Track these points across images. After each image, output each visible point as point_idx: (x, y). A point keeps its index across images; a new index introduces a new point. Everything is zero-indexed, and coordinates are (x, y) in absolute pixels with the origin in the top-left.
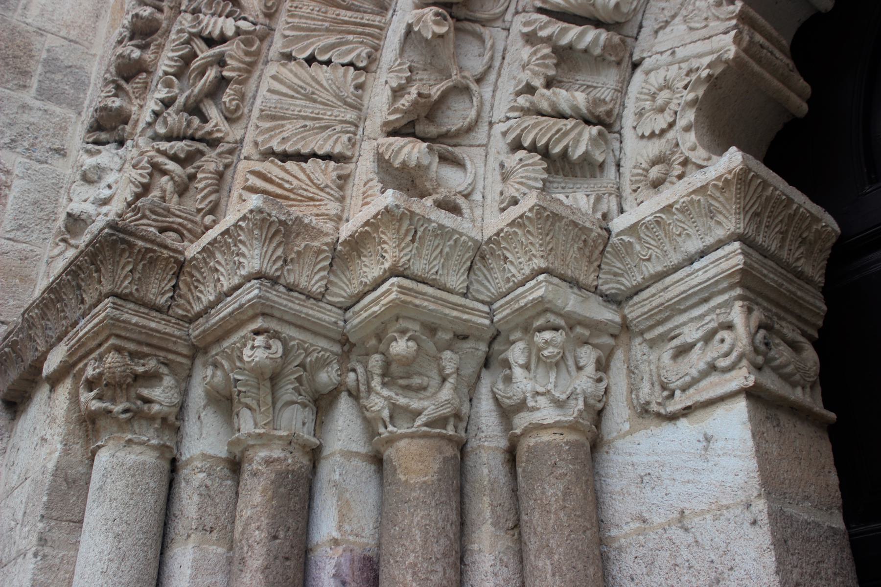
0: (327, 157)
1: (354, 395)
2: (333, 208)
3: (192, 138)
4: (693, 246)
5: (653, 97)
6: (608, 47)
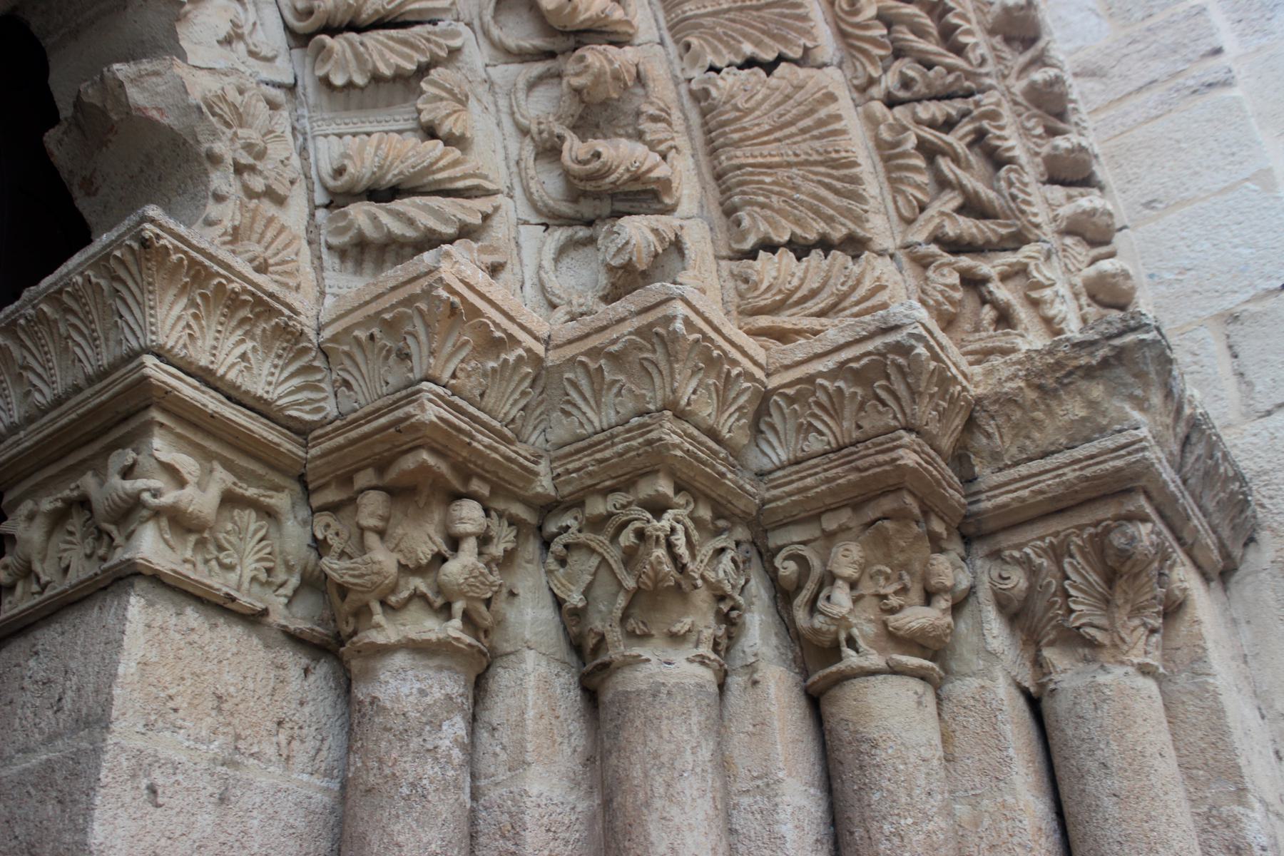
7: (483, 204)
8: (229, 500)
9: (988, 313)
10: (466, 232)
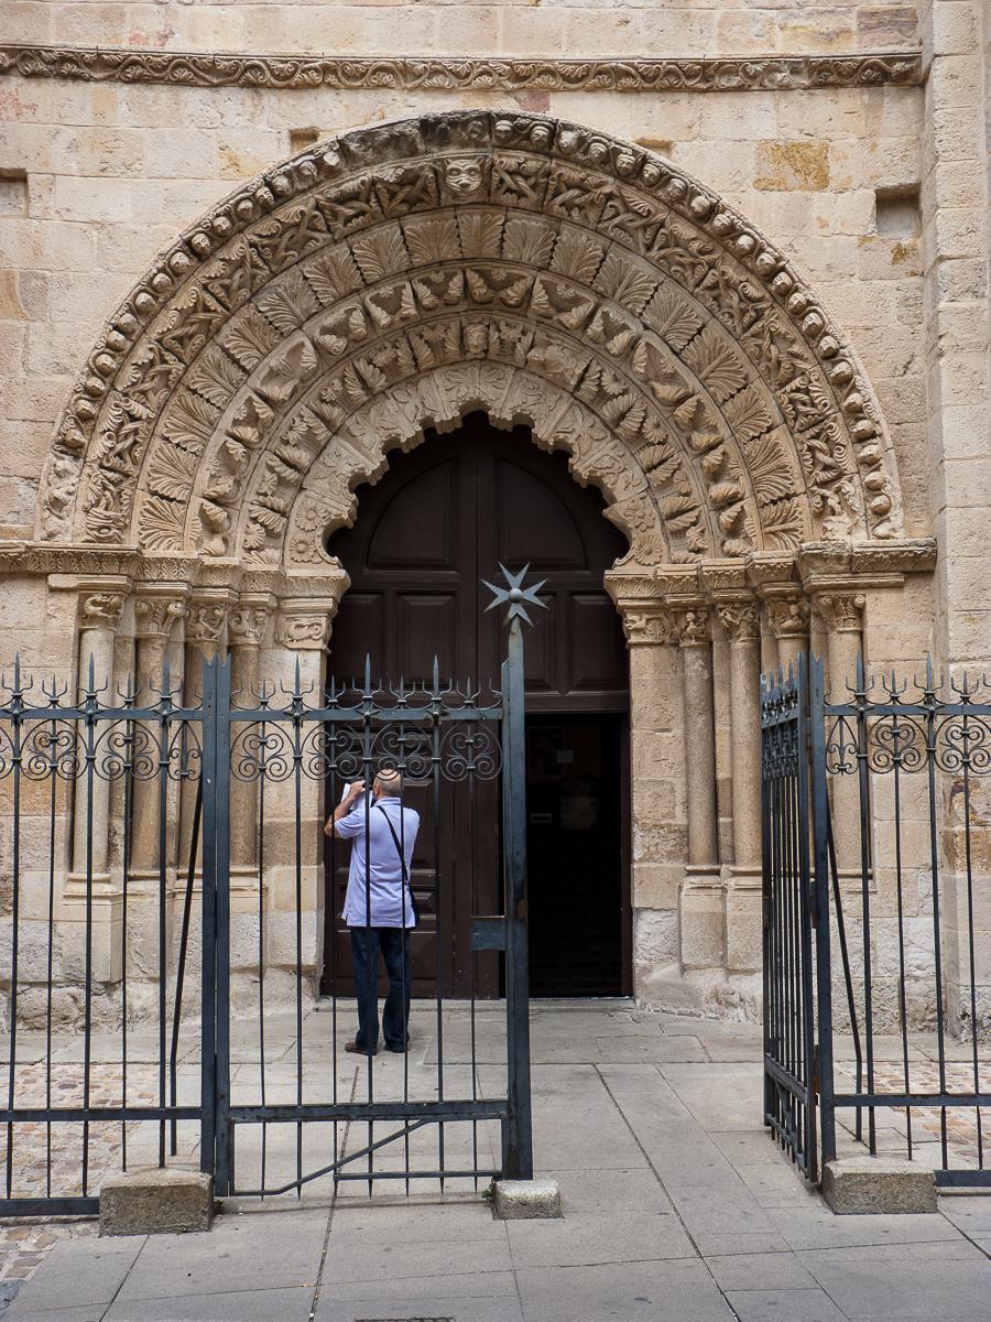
0: (179, 502)
1: (187, 619)
2: (180, 529)
3: (120, 473)
4: (316, 594)
5: (307, 512)
6: (297, 480)
7: (695, 513)
8: (648, 621)
9: (829, 509)
10: (694, 524)
